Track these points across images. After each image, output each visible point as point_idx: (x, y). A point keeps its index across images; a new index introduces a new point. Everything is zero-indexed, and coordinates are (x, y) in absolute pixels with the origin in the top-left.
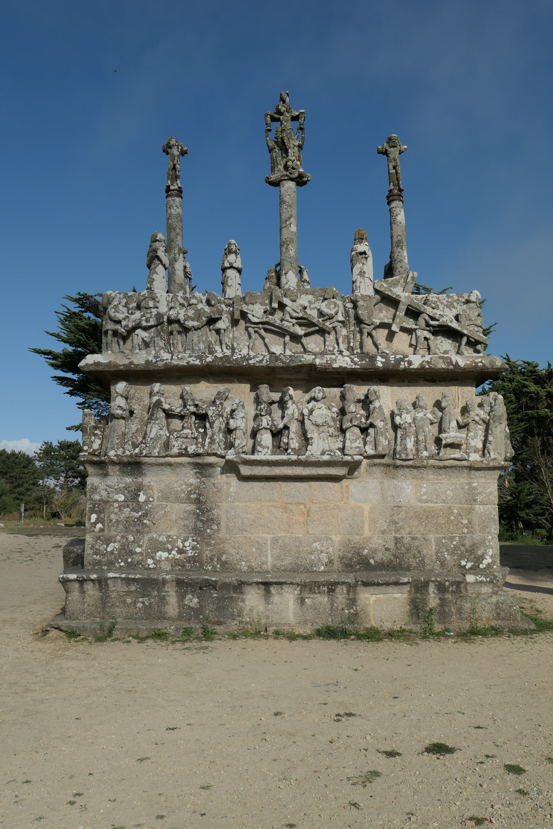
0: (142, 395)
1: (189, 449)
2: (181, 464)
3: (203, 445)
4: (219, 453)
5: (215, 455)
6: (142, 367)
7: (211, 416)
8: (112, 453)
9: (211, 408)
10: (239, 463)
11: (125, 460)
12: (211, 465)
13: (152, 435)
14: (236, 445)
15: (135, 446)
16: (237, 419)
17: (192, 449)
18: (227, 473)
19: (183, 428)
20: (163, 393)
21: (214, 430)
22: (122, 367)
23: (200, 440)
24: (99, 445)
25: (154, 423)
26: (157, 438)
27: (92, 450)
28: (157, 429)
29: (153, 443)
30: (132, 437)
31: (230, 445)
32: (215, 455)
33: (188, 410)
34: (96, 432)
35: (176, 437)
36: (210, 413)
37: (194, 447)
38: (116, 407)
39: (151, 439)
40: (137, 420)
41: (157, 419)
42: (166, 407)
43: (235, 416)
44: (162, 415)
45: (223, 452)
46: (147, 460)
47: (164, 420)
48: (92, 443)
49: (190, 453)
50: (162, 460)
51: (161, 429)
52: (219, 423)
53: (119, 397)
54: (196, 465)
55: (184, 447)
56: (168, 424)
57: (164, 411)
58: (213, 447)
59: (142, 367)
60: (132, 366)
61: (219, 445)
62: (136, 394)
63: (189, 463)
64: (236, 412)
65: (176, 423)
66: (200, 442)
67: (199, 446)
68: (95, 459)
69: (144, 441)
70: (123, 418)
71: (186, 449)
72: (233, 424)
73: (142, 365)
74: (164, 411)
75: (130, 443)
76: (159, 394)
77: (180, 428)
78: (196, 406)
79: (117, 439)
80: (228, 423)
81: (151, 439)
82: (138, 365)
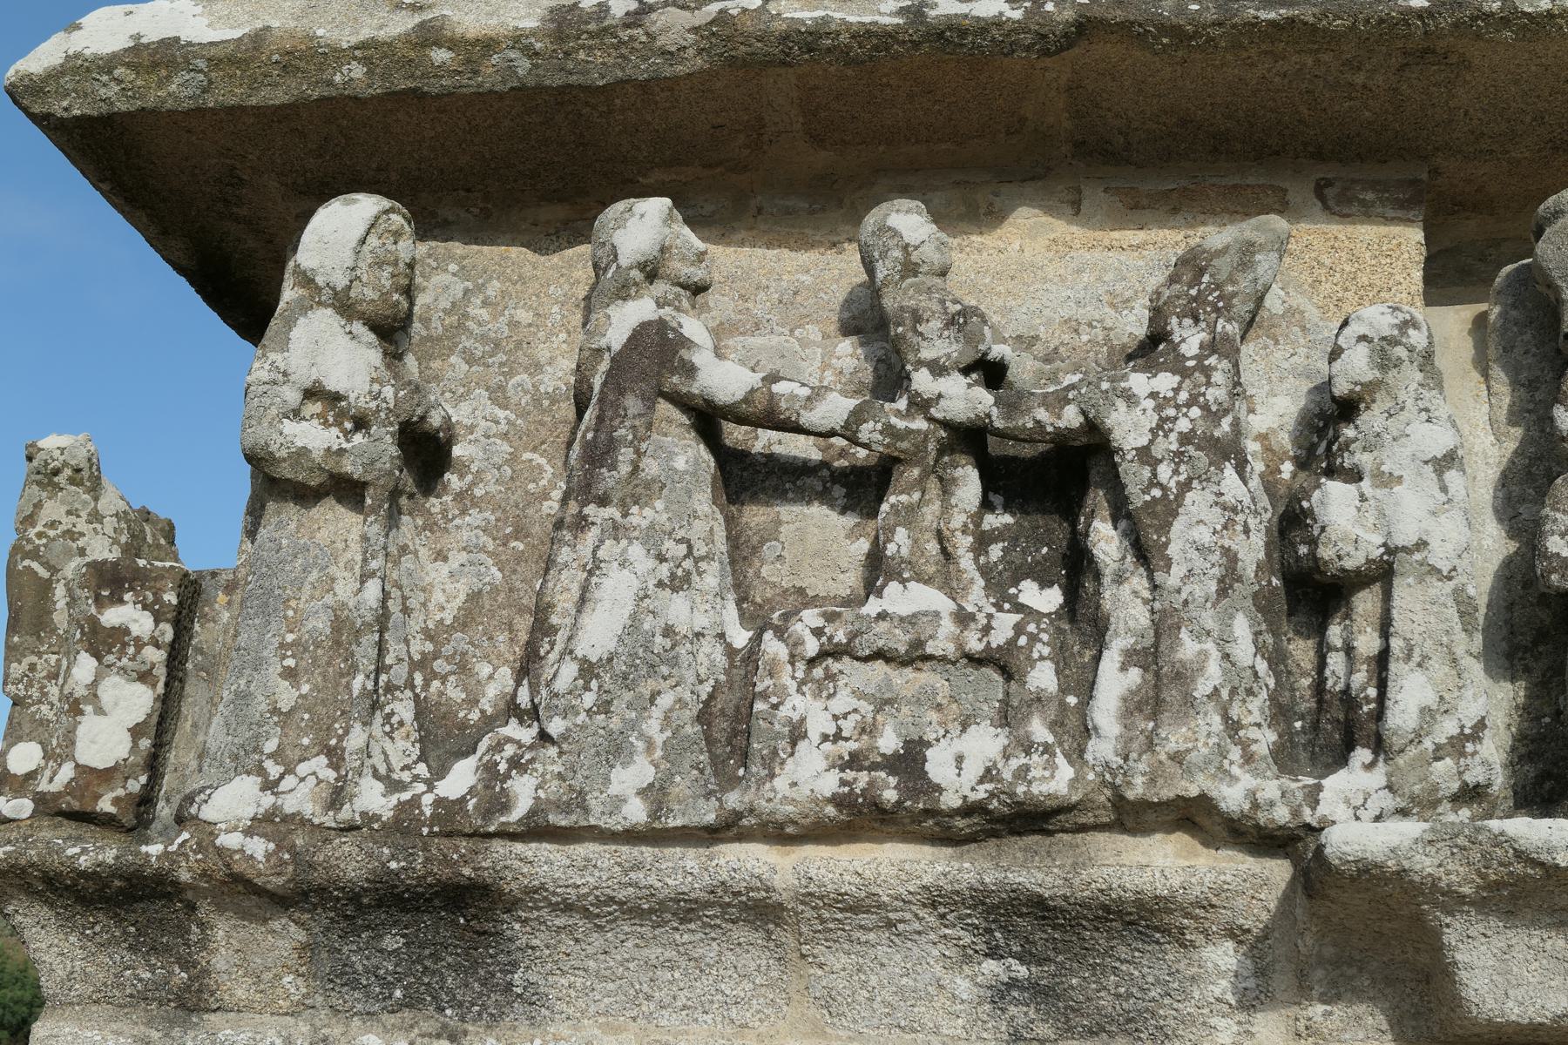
0: (524, 316)
1: (938, 765)
2: (856, 908)
3: (1076, 731)
4: (1232, 798)
5: (1194, 817)
6: (523, 65)
7: (1144, 454)
8: (232, 803)
9: (1139, 382)
10: (1453, 901)
11: (351, 862)
12: (1146, 920)
13: (599, 633)
14: (1402, 714)
15: (442, 738)
16: (1387, 480)
17: (964, 763)
18: (1302, 991)
19: (878, 569)
20: (697, 274)
21: (1173, 579)
22: (358, 71)
23: (1043, 677)
24: (136, 732)
25: (616, 531)
26: (647, 656)
27: (67, 772)
28: (644, 585)
29: (604, 707)
30: (424, 663)
31: (1338, 728)
32: (1194, 817)
33: (921, 405)
34: (112, 617)
35: (812, 647)
36: (1129, 428)
37: (984, 743)
38: (292, 396)
39: (588, 670)
40: (475, 517)
41: (639, 491)
42: (724, 378)
43: (1364, 459)
44: (685, 455)
45: (1270, 789)
46: (546, 863)
47: (703, 501)
48: (75, 708)
49: (951, 801)
50: (683, 870)
51: (678, 583)
52: (1216, 527)
53: (324, 321)
54: (1009, 920)
55: (889, 742)
56: (741, 552)
57: (707, 419)
58: (1174, 738)
59: (523, 65)
60: (440, 55)
61: (1233, 726)
62: (476, 310)
63: (935, 899)
64: (1371, 419)
65: (814, 542)
66: (1039, 699)
67: (1039, 730)
68: (91, 853)
69: (524, 698)
70: (348, 490)
71: (909, 762)
72: (1346, 521)
73: (518, 40)
74: (707, 419)
75: (404, 709)
76: (660, 287)
77: (851, 580)
78: (992, 373)
79: (290, 674)
80: (1293, 521)
81: (588, 670)
82: (488, 45)
